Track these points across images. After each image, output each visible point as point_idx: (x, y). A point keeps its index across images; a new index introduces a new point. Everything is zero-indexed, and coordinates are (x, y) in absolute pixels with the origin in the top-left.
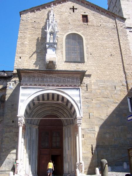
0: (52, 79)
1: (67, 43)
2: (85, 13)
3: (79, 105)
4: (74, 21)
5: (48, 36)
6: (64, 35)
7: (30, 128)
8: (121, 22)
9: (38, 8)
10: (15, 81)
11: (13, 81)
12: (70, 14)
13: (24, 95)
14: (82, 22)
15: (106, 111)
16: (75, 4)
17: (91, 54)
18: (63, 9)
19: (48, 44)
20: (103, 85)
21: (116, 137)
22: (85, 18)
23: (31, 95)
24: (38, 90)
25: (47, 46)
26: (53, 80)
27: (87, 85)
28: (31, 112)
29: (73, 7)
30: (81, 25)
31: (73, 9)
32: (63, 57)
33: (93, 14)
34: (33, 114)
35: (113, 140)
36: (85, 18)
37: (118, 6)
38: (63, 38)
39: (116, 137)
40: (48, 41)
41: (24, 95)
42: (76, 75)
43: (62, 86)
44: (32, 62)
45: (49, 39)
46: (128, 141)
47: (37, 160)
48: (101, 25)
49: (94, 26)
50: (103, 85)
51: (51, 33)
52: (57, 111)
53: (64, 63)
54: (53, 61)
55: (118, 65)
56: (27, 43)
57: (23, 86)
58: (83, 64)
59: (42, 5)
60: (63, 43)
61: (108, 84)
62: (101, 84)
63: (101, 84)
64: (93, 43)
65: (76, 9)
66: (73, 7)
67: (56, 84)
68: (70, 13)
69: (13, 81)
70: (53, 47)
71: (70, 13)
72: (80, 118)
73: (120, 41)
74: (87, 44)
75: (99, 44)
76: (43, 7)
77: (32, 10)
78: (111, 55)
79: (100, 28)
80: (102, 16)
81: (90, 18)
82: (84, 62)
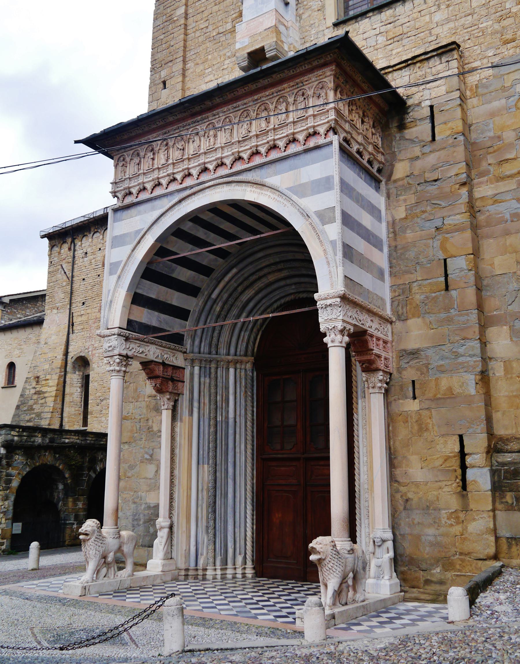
0: (215, 136)
23: (144, 230)
27: (432, 107)
34: (218, 309)
47: (249, 507)
72: (329, 302)
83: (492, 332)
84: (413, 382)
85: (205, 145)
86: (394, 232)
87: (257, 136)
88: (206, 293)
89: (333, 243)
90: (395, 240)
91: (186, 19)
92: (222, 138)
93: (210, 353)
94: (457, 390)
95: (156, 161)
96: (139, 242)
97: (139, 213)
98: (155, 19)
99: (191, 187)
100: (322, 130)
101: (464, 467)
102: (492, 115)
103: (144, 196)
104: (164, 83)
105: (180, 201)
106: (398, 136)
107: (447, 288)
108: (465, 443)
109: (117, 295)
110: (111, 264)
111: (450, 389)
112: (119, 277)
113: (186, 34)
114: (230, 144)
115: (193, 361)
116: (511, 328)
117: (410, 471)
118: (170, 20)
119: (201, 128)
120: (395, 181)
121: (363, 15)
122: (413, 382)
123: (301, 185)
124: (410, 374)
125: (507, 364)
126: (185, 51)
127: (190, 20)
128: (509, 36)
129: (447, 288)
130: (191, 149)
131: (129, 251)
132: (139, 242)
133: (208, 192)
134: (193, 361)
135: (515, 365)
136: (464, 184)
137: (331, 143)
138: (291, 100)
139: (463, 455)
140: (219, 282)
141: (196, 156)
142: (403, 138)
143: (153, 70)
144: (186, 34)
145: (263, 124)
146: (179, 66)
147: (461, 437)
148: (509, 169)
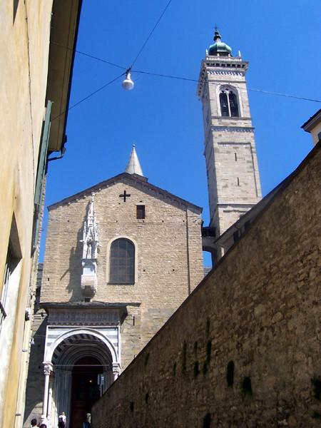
1: (113, 254)
3: (116, 348)
5: (85, 247)
6: (108, 242)
7: (60, 375)
8: (195, 215)
9: (73, 199)
10: (42, 313)
12: (118, 206)
13: (50, 337)
16: (127, 186)
19: (85, 260)
22: (141, 211)
25: (83, 264)
26: (87, 317)
30: (134, 223)
31: (125, 196)
32: (105, 276)
36: (141, 211)
40: (84, 257)
41: (50, 337)
42: (114, 310)
43: (96, 325)
45: (86, 254)
49: (153, 223)
51: (90, 243)
53: (106, 286)
55: (181, 285)
56: (57, 257)
59: (78, 194)
61: (164, 314)
62: (155, 314)
63: (155, 314)
65: (129, 195)
67: (90, 322)
73: (189, 247)
75: (157, 254)
76: (81, 195)
77: (65, 202)
80: (168, 206)
82: (133, 283)
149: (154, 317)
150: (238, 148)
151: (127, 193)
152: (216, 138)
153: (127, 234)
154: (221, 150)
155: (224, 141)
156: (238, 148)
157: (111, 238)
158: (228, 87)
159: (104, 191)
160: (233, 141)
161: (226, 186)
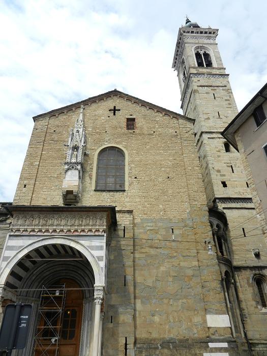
0: (61, 221)
2: (132, 115)
4: (115, 128)
11: (8, 224)
12: (108, 118)
13: (10, 248)
14: (125, 130)
15: (155, 271)
17: (136, 178)
18: (100, 112)
20: (152, 226)
21: (172, 321)
22: (131, 123)
24: (36, 239)
28: (28, 275)
29: (115, 107)
30: (124, 134)
32: (91, 183)
33: (145, 116)
34: (34, 278)
35: (167, 327)
37: (193, 101)
38: (94, 155)
39: (172, 321)
41: (10, 248)
44: (42, 192)
46: (195, 331)
48: (154, 132)
50: (152, 226)
52: (75, 272)
53: (92, 193)
54: (72, 191)
55: (178, 193)
57: (12, 234)
58: (121, 193)
60: (93, 162)
62: (149, 224)
63: (149, 224)
64: (141, 161)
66: (115, 107)
68: (109, 117)
69: (8, 224)
70: (75, 169)
71: (109, 117)
72: (99, 288)
74: (131, 162)
78: (168, 177)
79: (154, 136)
81: (139, 123)
83: (137, 300)
84: (112, 317)
85: (56, 222)
86: (110, 263)
87: (78, 226)
88: (32, 272)
89: (102, 268)
90: (109, 266)
91: (39, 166)
92: (63, 222)
93: (26, 296)
94: (126, 321)
95: (34, 222)
96: (20, 251)
97: (23, 239)
98: (25, 161)
99: (48, 236)
100: (101, 230)
101: (126, 349)
102: (140, 233)
103: (24, 233)
104: (25, 186)
105: (43, 240)
106: (113, 233)
107: (125, 285)
108: (127, 340)
109: (5, 270)
110: (4, 257)
111: (123, 320)
112: (8, 264)
113: (38, 172)
114: (66, 225)
115: (20, 299)
116: (142, 300)
117: (109, 350)
118: (32, 164)
119: (56, 216)
120: (112, 247)
121: (104, 191)
122: (112, 317)
123: (92, 246)
124: (111, 314)
125: (140, 312)
126: (36, 177)
127: (40, 168)
128: (146, 213)
129: (125, 285)
130: (50, 222)
131: (15, 254)
132: (20, 251)
133: (55, 239)
134: (20, 299)
135: (142, 313)
136: (132, 253)
137: (103, 236)
138: (91, 218)
139: (126, 344)
140: (38, 268)
141: (52, 225)
142: (115, 234)
143: (20, 179)
144: (38, 172)
145: (81, 222)
146: (33, 182)
147: (126, 338)
148: (143, 250)
149: (148, 228)
150: (216, 90)
151: (116, 108)
152: (196, 82)
153: (117, 143)
154: (200, 92)
155: (203, 85)
156: (216, 90)
157: (100, 146)
158: (202, 48)
159: (94, 106)
160: (209, 84)
161: (208, 118)
